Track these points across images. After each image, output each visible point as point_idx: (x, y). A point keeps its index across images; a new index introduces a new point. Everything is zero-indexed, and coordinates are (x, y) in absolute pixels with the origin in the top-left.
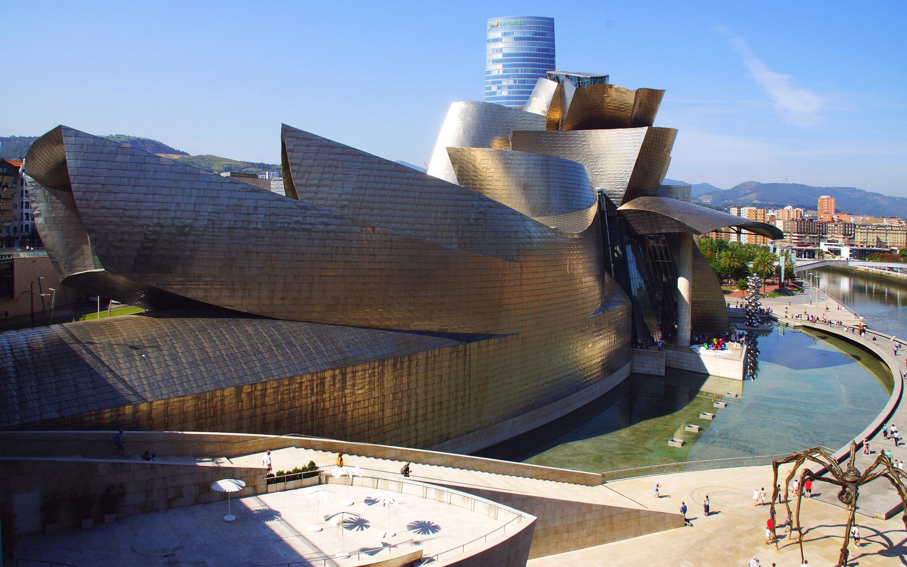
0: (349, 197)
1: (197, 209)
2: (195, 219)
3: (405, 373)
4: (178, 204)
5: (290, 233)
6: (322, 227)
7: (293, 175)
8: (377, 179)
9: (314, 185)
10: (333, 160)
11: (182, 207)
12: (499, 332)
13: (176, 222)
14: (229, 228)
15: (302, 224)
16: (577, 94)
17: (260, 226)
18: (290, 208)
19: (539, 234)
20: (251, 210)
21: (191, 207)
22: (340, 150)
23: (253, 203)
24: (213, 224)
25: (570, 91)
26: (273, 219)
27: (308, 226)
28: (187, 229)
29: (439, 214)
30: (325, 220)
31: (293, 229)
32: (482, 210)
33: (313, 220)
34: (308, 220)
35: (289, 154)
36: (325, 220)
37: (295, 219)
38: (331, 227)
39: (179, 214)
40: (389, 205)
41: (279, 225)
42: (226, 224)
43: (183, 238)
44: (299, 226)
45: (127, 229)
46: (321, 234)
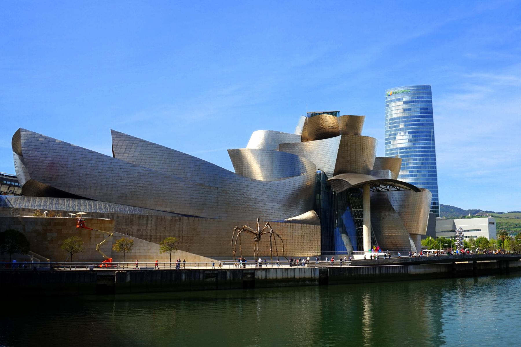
3: (145, 222)
4: (61, 156)
6: (118, 167)
11: (63, 157)
12: (202, 216)
13: (60, 162)
17: (92, 165)
20: (90, 159)
21: (66, 157)
22: (134, 139)
27: (112, 166)
33: (114, 164)
34: (112, 164)
39: (61, 159)
42: (79, 164)
45: (41, 164)
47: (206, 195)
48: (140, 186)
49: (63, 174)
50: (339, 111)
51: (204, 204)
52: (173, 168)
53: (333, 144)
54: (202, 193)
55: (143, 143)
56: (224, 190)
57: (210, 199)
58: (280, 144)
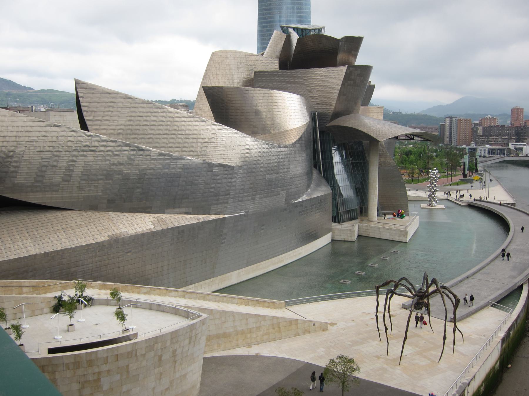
0: (122, 127)
1: (18, 140)
2: (16, 147)
5: (82, 153)
6: (102, 148)
7: (84, 113)
8: (141, 114)
9: (98, 120)
10: (111, 102)
11: (7, 139)
14: (41, 151)
15: (89, 146)
16: (299, 41)
17: (60, 150)
18: (81, 136)
19: (256, 147)
20: (55, 139)
21: (13, 139)
23: (55, 134)
24: (29, 149)
25: (295, 37)
26: (69, 144)
27: (93, 149)
28: (12, 153)
29: (185, 136)
30: (105, 143)
31: (83, 151)
32: (213, 132)
33: (96, 144)
34: (93, 144)
35: (81, 99)
36: (105, 143)
37: (85, 144)
38: (109, 148)
39: (5, 144)
40: (150, 132)
41: (74, 148)
42: (38, 149)
43: (9, 160)
44: (86, 148)
46: (102, 153)
47: (230, 180)
48: (140, 179)
49: (12, 169)
50: (324, 27)
51: (229, 194)
52: (180, 141)
53: (333, 77)
54: (225, 178)
55: (130, 100)
56: (250, 168)
57: (234, 186)
58: (255, 72)
